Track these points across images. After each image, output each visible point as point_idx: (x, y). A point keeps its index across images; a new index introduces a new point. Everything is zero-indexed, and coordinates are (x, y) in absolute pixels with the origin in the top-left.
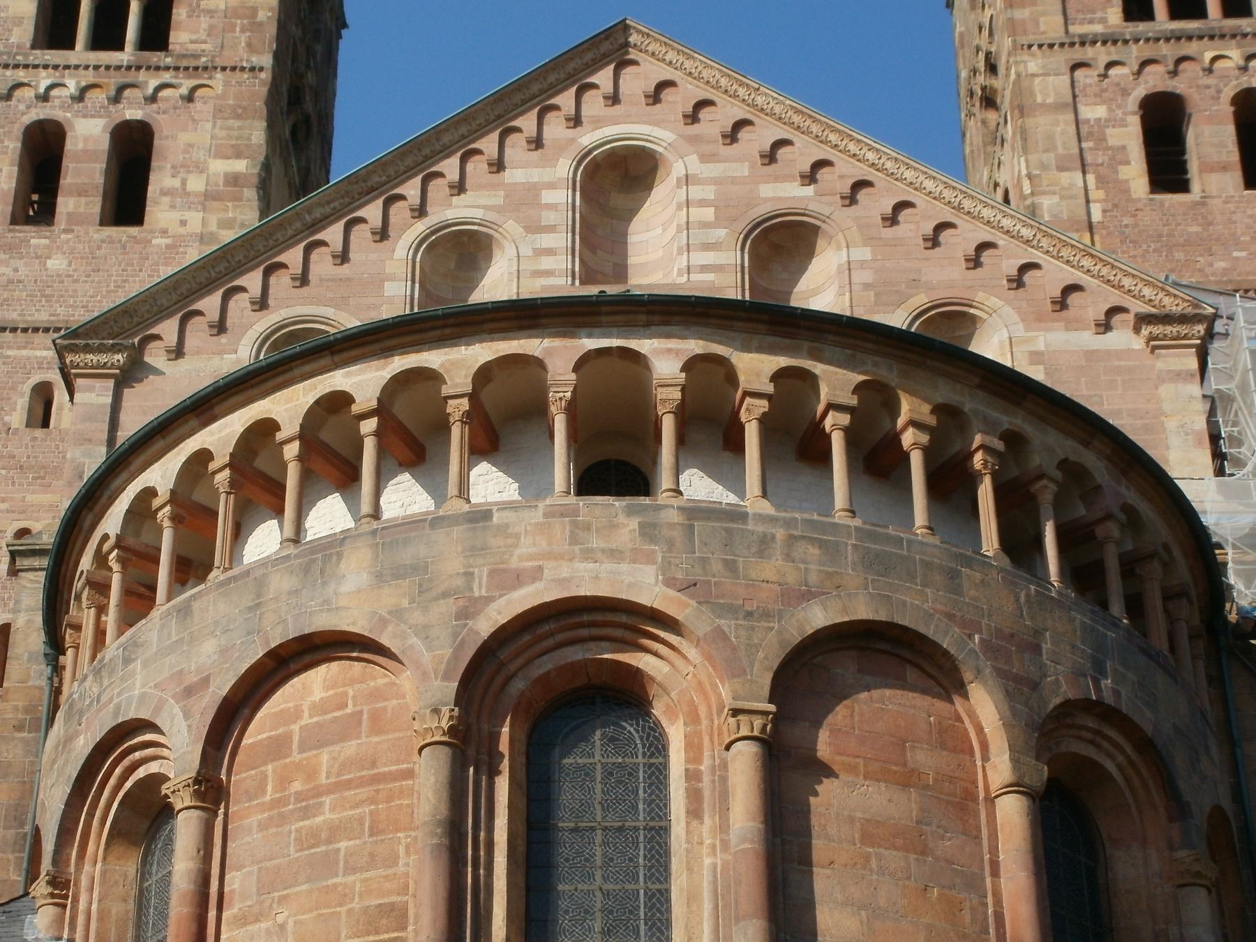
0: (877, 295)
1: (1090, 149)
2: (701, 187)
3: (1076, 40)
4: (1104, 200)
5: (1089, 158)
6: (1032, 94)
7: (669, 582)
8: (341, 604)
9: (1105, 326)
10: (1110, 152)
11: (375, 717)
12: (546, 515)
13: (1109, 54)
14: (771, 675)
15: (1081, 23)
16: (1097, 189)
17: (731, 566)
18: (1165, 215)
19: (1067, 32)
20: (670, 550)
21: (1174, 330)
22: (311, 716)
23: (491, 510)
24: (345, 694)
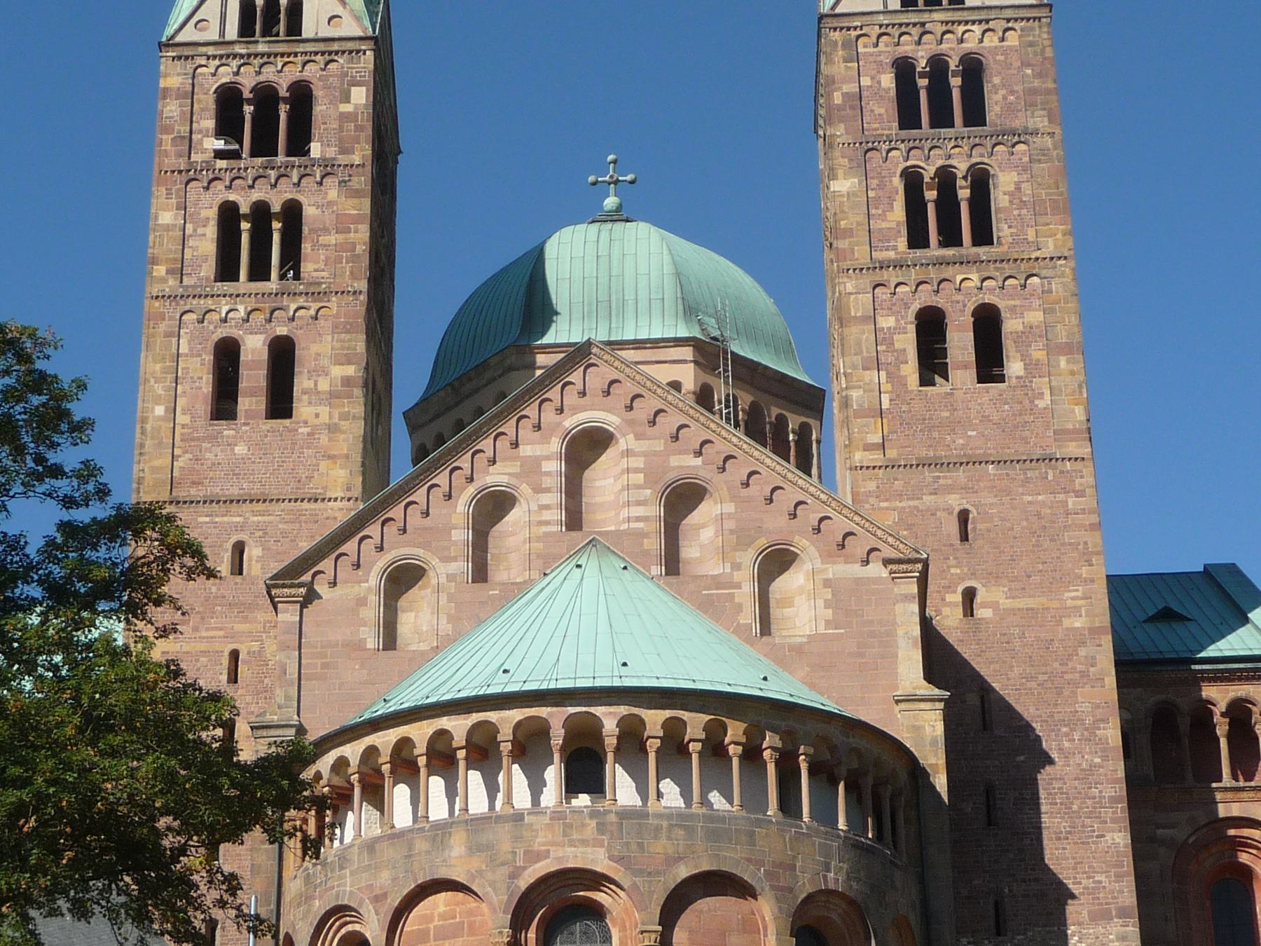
0: (737, 537)
1: (884, 351)
2: (637, 458)
3: (877, 265)
4: (891, 392)
5: (882, 359)
6: (849, 309)
7: (611, 858)
8: (452, 863)
9: (866, 562)
10: (896, 354)
11: (471, 925)
12: (551, 819)
13: (897, 277)
14: (660, 908)
15: (881, 250)
16: (887, 382)
17: (640, 845)
18: (927, 403)
19: (871, 259)
20: (612, 839)
21: (905, 567)
22: (439, 921)
23: (523, 814)
24: (455, 911)
